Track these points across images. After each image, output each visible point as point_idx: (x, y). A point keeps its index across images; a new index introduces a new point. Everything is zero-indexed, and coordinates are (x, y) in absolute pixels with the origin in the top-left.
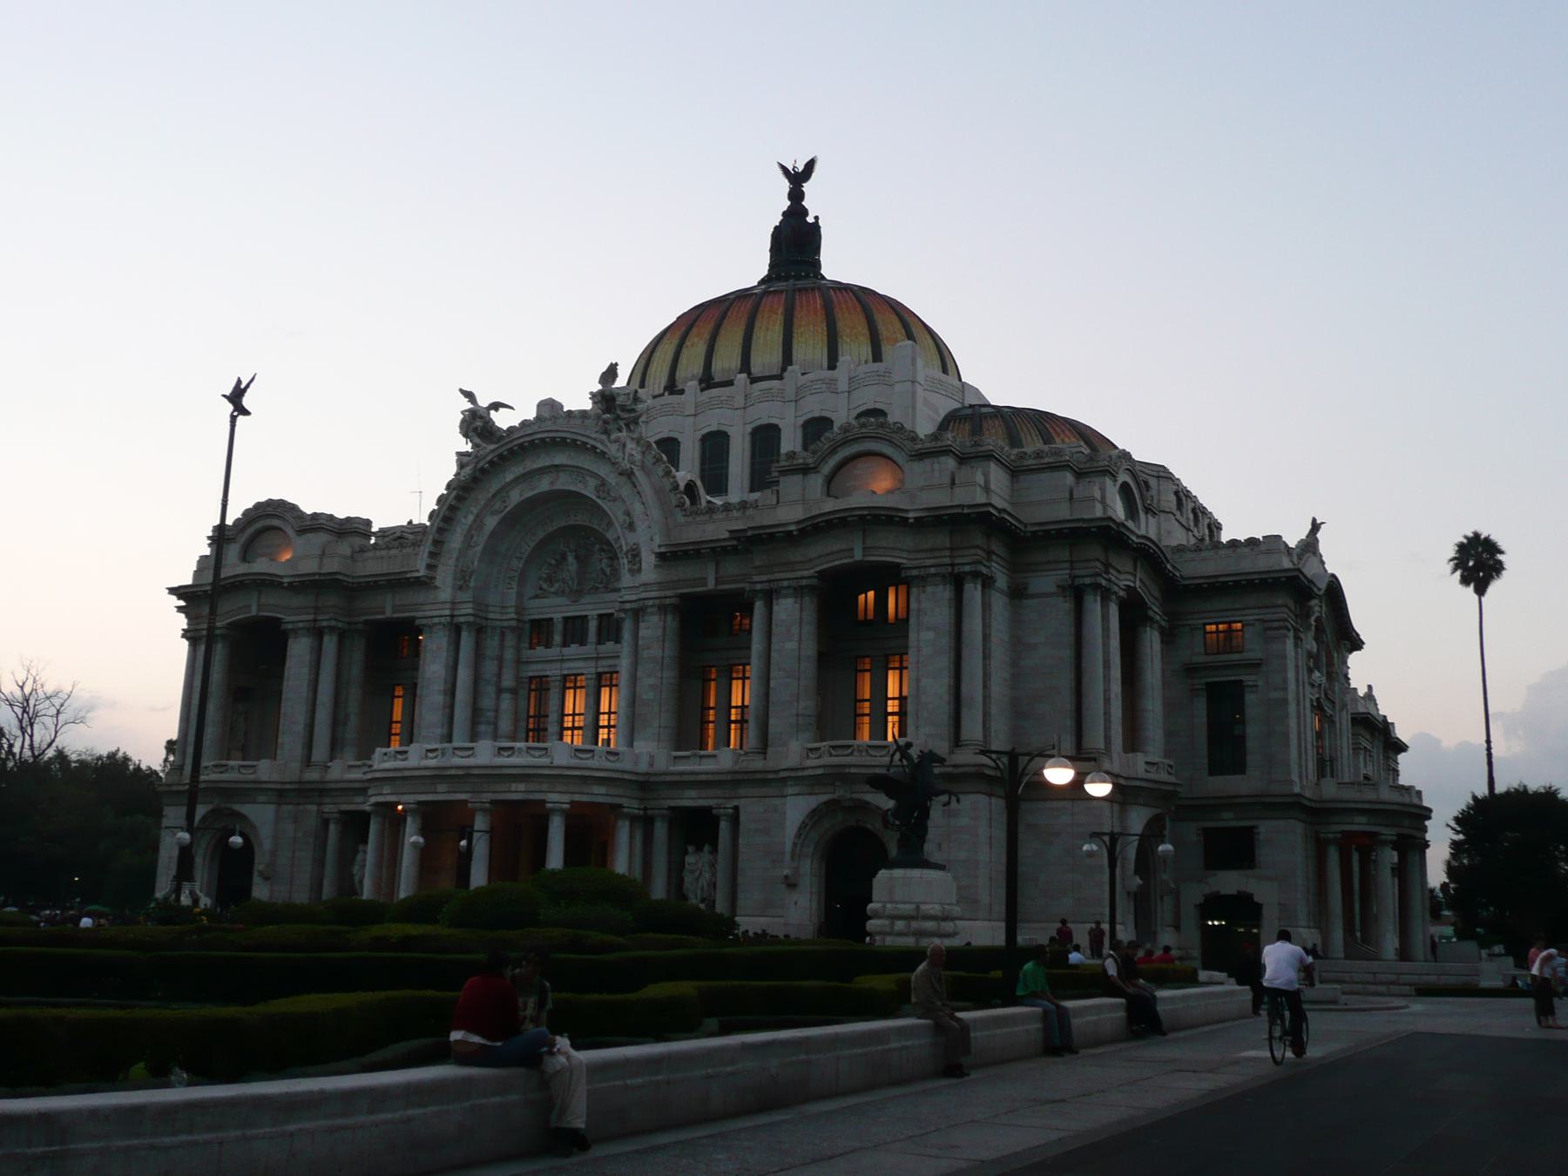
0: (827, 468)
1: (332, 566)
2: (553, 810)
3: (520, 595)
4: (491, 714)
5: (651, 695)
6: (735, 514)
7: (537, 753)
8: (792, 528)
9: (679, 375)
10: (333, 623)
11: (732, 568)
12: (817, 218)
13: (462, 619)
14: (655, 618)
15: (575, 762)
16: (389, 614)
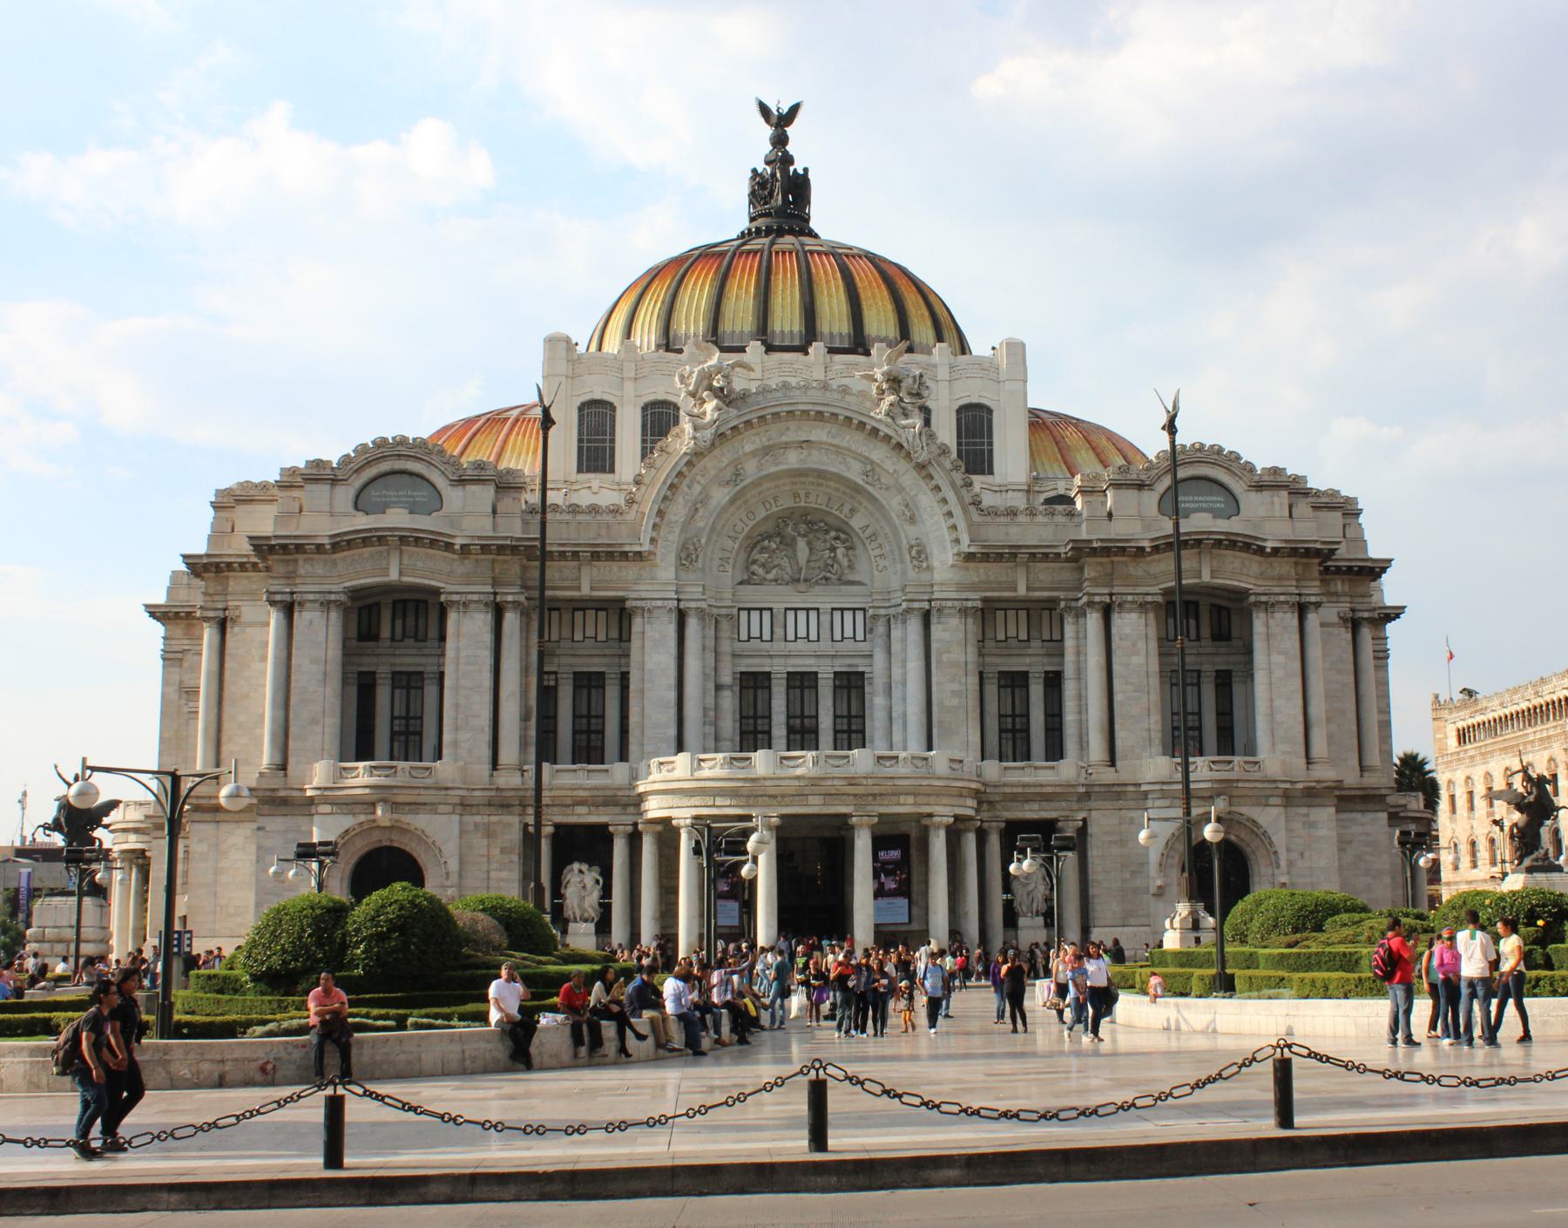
1: (514, 529)
4: (712, 713)
5: (955, 702)
8: (1146, 544)
9: (726, 326)
10: (522, 598)
11: (1046, 574)
12: (806, 170)
13: (693, 605)
14: (954, 621)
16: (585, 591)
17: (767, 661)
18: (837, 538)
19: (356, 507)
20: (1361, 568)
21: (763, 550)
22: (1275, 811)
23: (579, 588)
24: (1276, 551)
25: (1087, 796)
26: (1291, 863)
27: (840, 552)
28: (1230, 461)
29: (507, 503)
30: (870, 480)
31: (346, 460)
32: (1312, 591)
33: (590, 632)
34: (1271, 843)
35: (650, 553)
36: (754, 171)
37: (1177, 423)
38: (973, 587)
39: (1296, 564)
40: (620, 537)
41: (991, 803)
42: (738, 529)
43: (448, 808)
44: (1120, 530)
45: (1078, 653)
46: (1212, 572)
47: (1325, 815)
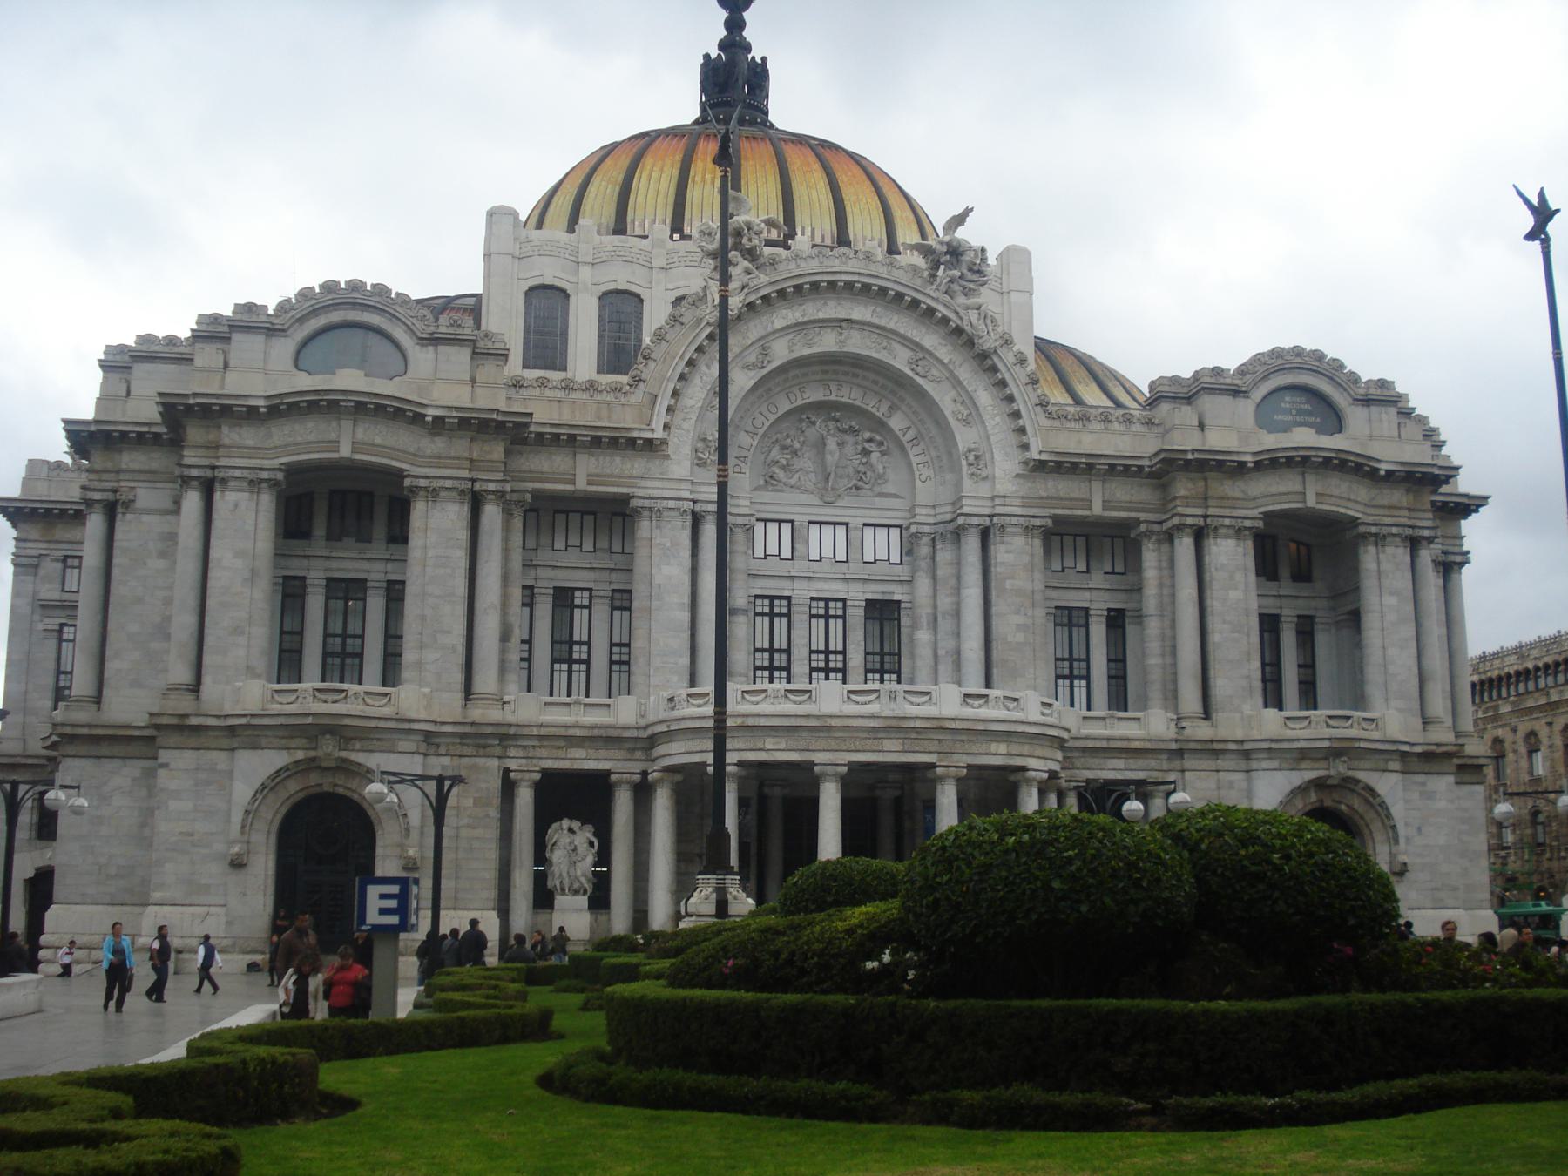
0: (1258, 394)
2: (1029, 781)
5: (1020, 637)
6: (1116, 426)
7: (1012, 705)
8: (1248, 458)
10: (508, 488)
11: (1123, 492)
12: (764, 59)
14: (1019, 542)
15: (1042, 719)
16: (581, 484)
17: (786, 583)
18: (870, 440)
19: (296, 366)
20: (1457, 504)
21: (784, 448)
22: (1394, 778)
24: (1390, 473)
25: (1180, 753)
26: (1408, 839)
27: (875, 457)
28: (1333, 370)
29: (488, 371)
30: (919, 369)
31: (284, 306)
32: (1425, 522)
33: (574, 541)
34: (1389, 816)
35: (664, 442)
36: (707, 57)
37: (1551, 228)
38: (1042, 501)
39: (1408, 491)
40: (624, 418)
42: (758, 423)
43: (412, 746)
44: (1219, 440)
45: (1161, 586)
46: (1318, 494)
47: (1443, 784)
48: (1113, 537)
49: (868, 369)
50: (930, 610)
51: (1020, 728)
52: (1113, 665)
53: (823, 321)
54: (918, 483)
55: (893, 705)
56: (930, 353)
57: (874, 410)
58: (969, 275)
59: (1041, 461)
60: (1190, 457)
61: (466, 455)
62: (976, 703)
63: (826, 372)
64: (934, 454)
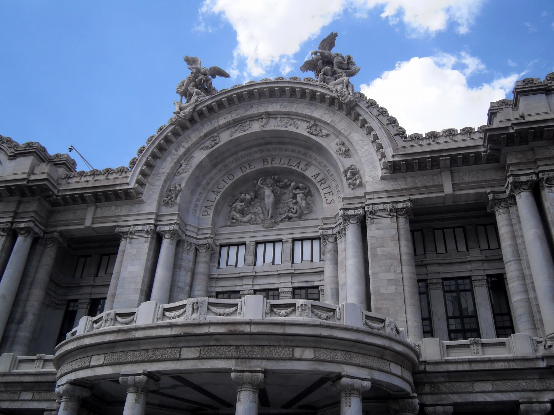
3: (214, 223)
5: (392, 289)
7: (324, 315)
10: (31, 225)
11: (467, 176)
13: (167, 228)
17: (238, 282)
18: (297, 188)
21: (242, 201)
23: (83, 224)
27: (299, 197)
41: (433, 384)
45: (514, 237)
48: (485, 225)
49: (288, 144)
50: (333, 286)
51: (325, 332)
52: (499, 318)
53: (251, 117)
54: (325, 205)
55: (195, 316)
56: (320, 121)
57: (296, 168)
58: (339, 71)
59: (394, 162)
60: (511, 131)
61: (14, 209)
62: (283, 312)
63: (261, 151)
64: (334, 185)
